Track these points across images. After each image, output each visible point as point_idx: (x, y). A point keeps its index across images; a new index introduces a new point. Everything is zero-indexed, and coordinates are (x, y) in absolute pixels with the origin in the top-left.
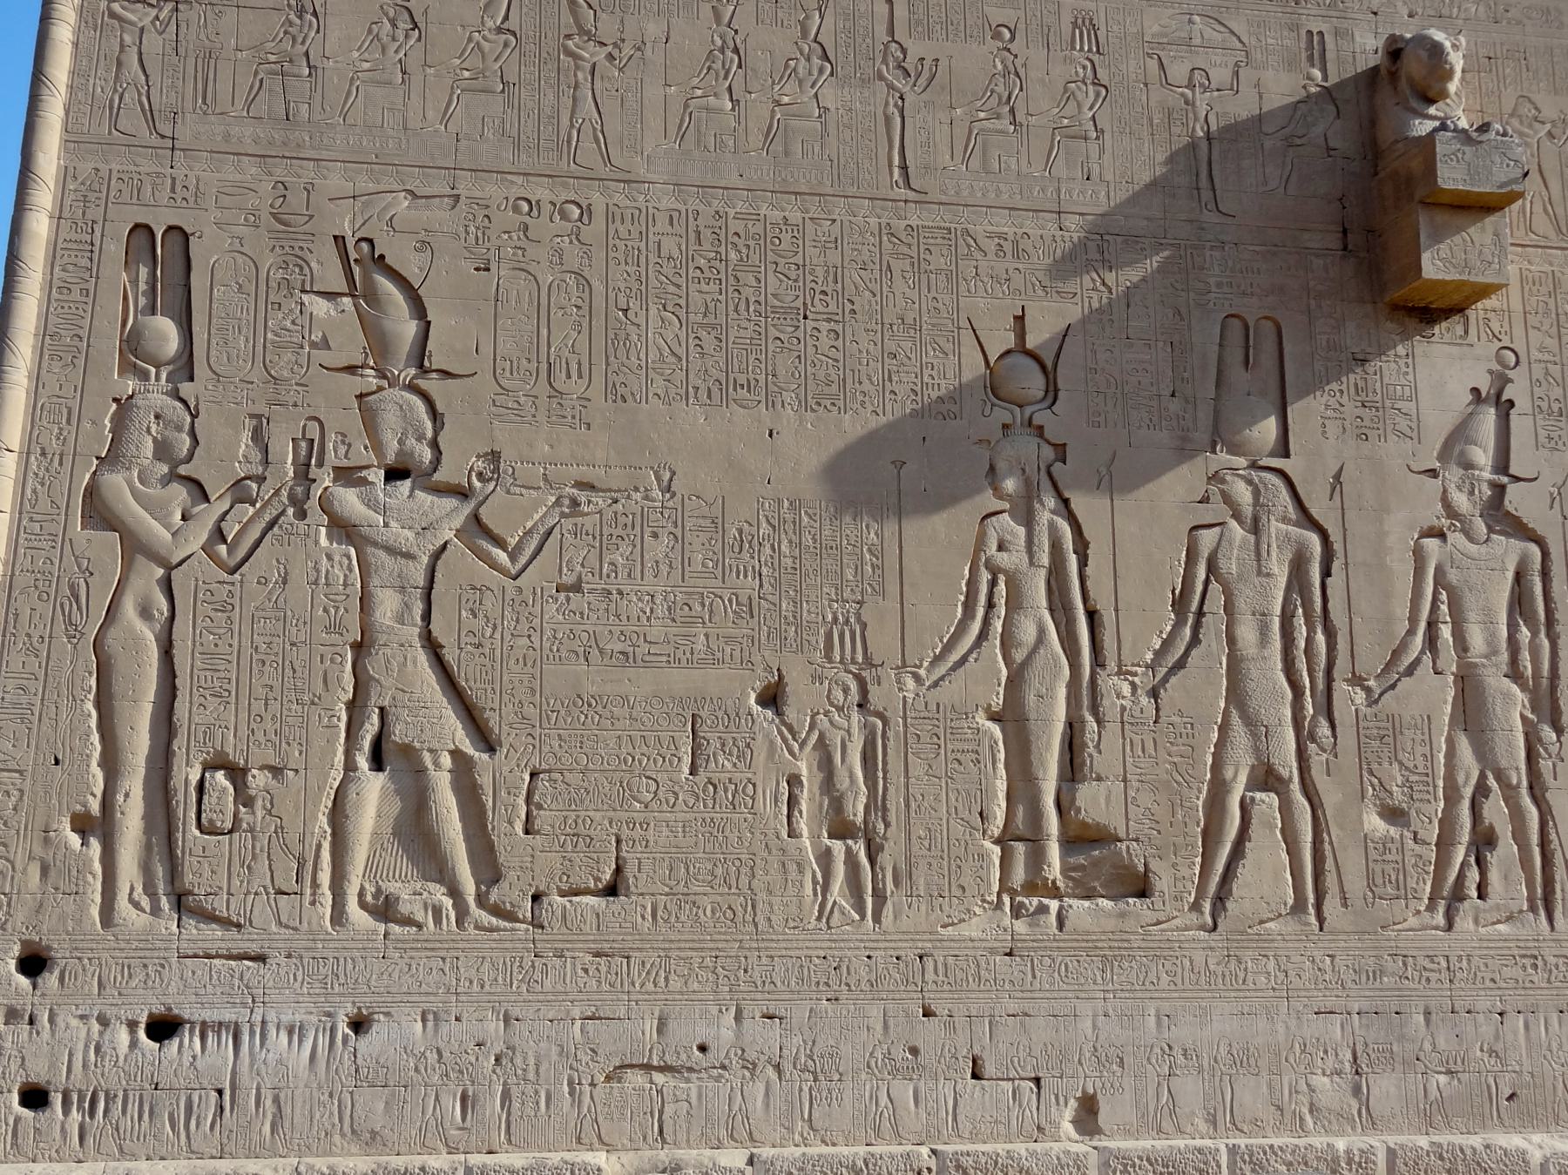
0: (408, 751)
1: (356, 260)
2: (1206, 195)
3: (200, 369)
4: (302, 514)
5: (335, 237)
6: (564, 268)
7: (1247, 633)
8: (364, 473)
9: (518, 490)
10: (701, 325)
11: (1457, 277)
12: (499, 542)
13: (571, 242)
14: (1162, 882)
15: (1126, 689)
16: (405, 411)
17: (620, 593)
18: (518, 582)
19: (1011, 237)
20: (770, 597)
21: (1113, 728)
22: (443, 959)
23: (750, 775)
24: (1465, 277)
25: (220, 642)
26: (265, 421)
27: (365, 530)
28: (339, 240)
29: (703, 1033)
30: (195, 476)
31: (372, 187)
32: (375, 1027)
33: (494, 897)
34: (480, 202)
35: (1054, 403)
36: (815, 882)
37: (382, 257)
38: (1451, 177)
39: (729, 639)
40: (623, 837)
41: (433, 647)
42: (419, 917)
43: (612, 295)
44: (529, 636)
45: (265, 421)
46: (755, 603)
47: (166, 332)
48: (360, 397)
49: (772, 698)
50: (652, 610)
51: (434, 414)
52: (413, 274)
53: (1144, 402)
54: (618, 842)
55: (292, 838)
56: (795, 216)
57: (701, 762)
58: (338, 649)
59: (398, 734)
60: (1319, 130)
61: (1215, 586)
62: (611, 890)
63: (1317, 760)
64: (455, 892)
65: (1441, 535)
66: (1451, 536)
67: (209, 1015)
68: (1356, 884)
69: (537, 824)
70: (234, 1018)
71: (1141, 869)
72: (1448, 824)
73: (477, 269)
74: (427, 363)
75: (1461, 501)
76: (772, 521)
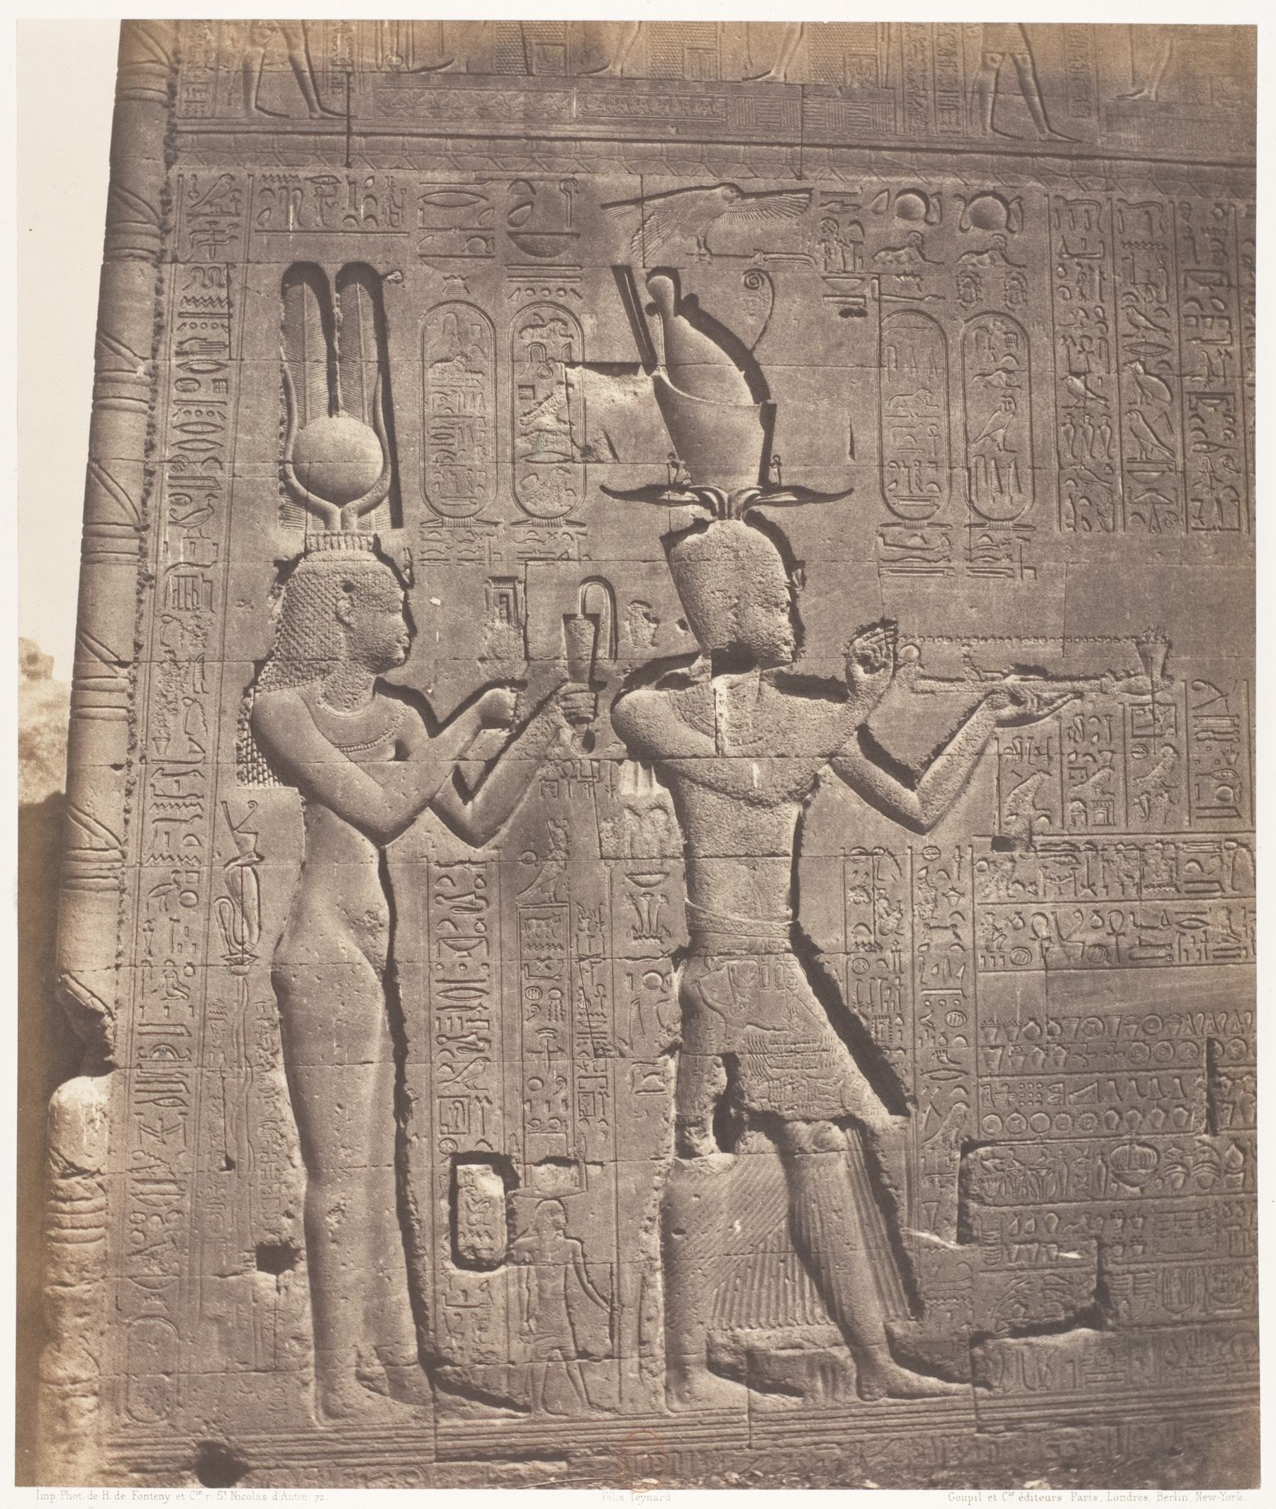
1: (652, 309)
3: (415, 509)
4: (589, 742)
13: (993, 260)
16: (740, 558)
17: (1092, 846)
25: (468, 960)
26: (520, 587)
28: (623, 273)
34: (847, 200)
37: (693, 299)
41: (803, 947)
43: (1061, 351)
45: (520, 587)
48: (671, 539)
50: (1142, 877)
51: (791, 564)
52: (745, 324)
55: (598, 1271)
73: (845, 314)
74: (773, 478)
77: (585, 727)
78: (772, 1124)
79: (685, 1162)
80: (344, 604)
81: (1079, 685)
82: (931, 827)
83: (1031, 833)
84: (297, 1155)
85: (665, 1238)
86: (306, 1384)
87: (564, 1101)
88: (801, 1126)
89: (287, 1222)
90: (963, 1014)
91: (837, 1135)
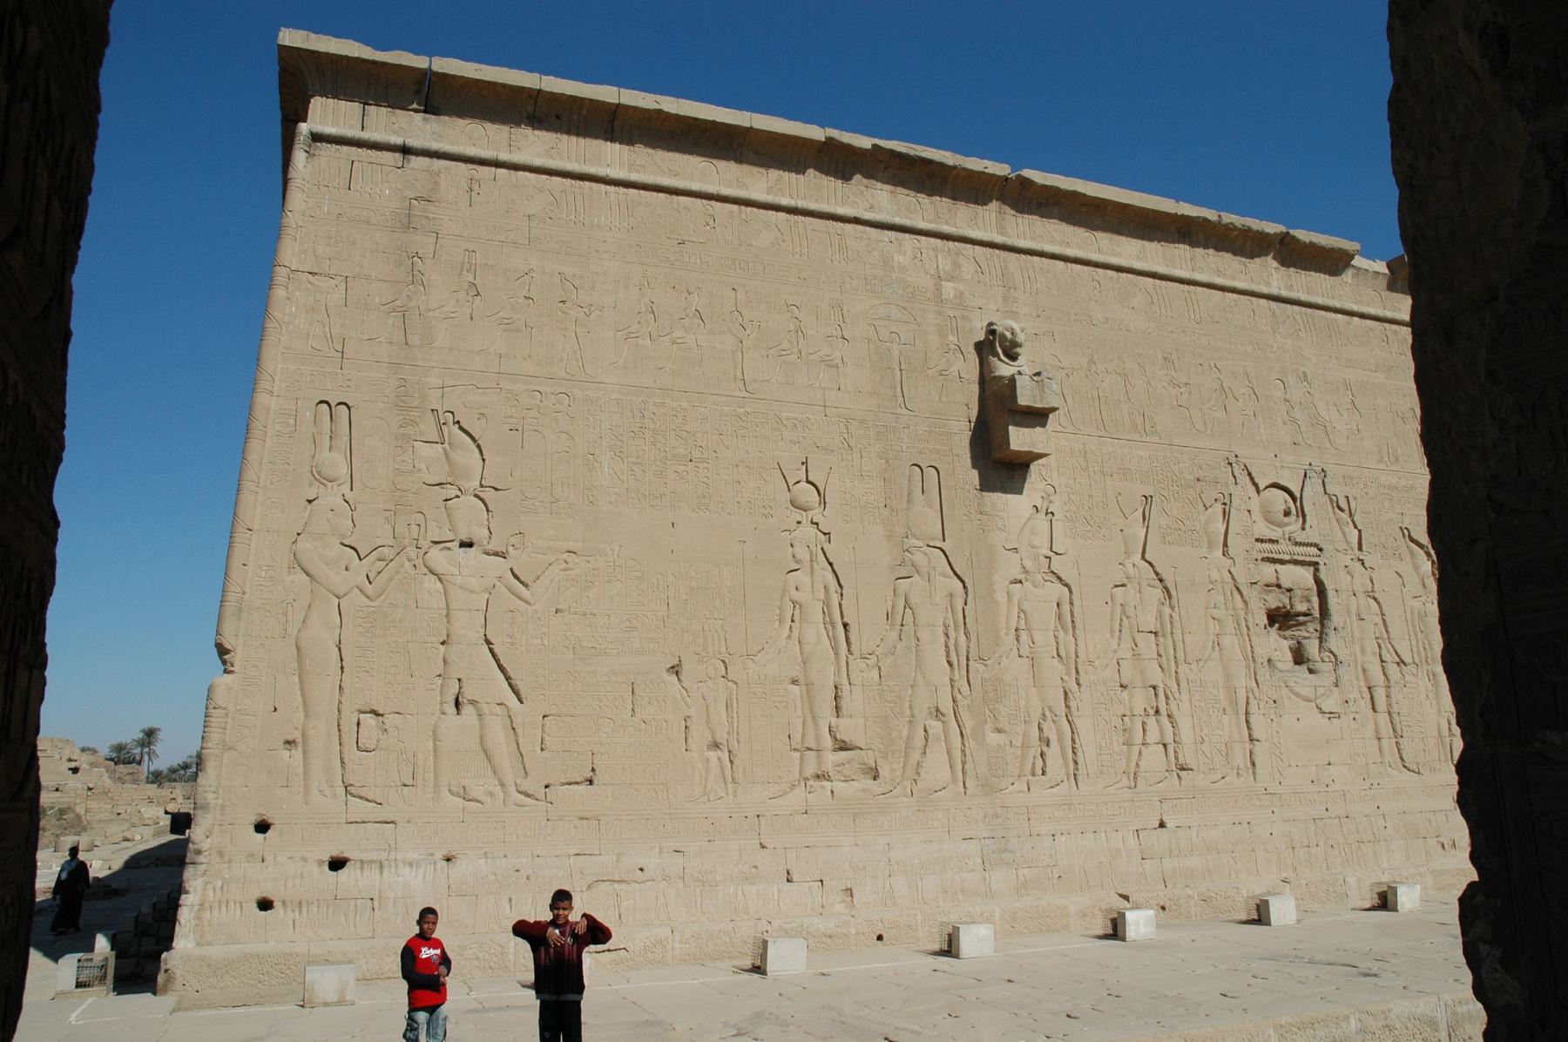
0: (472, 702)
1: (444, 424)
2: (900, 400)
5: (433, 410)
6: (560, 430)
7: (924, 635)
8: (448, 545)
9: (535, 555)
10: (635, 463)
11: (1027, 449)
12: (526, 585)
14: (884, 772)
18: (534, 607)
19: (800, 419)
22: (497, 822)
23: (664, 717)
24: (1031, 450)
26: (393, 513)
27: (450, 578)
29: (642, 862)
30: (352, 545)
31: (453, 383)
32: (459, 861)
33: (523, 789)
36: (701, 776)
37: (458, 422)
38: (1024, 399)
40: (595, 752)
41: (488, 642)
42: (482, 798)
44: (541, 638)
46: (666, 618)
47: (336, 462)
49: (676, 670)
50: (609, 624)
54: (593, 754)
56: (685, 405)
58: (435, 645)
59: (468, 693)
60: (955, 368)
61: (908, 610)
62: (591, 782)
63: (962, 703)
64: (502, 785)
65: (1021, 582)
66: (1025, 583)
67: (364, 856)
69: (548, 744)
70: (379, 858)
71: (874, 765)
72: (1026, 735)
73: (511, 430)
75: (1029, 564)
77: (413, 563)
78: (472, 702)
79: (442, 716)
80: (330, 516)
81: (587, 558)
82: (535, 604)
83: (570, 607)
84: (301, 708)
85: (435, 744)
86: (299, 793)
87: (400, 692)
88: (485, 705)
89: (296, 732)
90: (544, 669)
91: (498, 709)
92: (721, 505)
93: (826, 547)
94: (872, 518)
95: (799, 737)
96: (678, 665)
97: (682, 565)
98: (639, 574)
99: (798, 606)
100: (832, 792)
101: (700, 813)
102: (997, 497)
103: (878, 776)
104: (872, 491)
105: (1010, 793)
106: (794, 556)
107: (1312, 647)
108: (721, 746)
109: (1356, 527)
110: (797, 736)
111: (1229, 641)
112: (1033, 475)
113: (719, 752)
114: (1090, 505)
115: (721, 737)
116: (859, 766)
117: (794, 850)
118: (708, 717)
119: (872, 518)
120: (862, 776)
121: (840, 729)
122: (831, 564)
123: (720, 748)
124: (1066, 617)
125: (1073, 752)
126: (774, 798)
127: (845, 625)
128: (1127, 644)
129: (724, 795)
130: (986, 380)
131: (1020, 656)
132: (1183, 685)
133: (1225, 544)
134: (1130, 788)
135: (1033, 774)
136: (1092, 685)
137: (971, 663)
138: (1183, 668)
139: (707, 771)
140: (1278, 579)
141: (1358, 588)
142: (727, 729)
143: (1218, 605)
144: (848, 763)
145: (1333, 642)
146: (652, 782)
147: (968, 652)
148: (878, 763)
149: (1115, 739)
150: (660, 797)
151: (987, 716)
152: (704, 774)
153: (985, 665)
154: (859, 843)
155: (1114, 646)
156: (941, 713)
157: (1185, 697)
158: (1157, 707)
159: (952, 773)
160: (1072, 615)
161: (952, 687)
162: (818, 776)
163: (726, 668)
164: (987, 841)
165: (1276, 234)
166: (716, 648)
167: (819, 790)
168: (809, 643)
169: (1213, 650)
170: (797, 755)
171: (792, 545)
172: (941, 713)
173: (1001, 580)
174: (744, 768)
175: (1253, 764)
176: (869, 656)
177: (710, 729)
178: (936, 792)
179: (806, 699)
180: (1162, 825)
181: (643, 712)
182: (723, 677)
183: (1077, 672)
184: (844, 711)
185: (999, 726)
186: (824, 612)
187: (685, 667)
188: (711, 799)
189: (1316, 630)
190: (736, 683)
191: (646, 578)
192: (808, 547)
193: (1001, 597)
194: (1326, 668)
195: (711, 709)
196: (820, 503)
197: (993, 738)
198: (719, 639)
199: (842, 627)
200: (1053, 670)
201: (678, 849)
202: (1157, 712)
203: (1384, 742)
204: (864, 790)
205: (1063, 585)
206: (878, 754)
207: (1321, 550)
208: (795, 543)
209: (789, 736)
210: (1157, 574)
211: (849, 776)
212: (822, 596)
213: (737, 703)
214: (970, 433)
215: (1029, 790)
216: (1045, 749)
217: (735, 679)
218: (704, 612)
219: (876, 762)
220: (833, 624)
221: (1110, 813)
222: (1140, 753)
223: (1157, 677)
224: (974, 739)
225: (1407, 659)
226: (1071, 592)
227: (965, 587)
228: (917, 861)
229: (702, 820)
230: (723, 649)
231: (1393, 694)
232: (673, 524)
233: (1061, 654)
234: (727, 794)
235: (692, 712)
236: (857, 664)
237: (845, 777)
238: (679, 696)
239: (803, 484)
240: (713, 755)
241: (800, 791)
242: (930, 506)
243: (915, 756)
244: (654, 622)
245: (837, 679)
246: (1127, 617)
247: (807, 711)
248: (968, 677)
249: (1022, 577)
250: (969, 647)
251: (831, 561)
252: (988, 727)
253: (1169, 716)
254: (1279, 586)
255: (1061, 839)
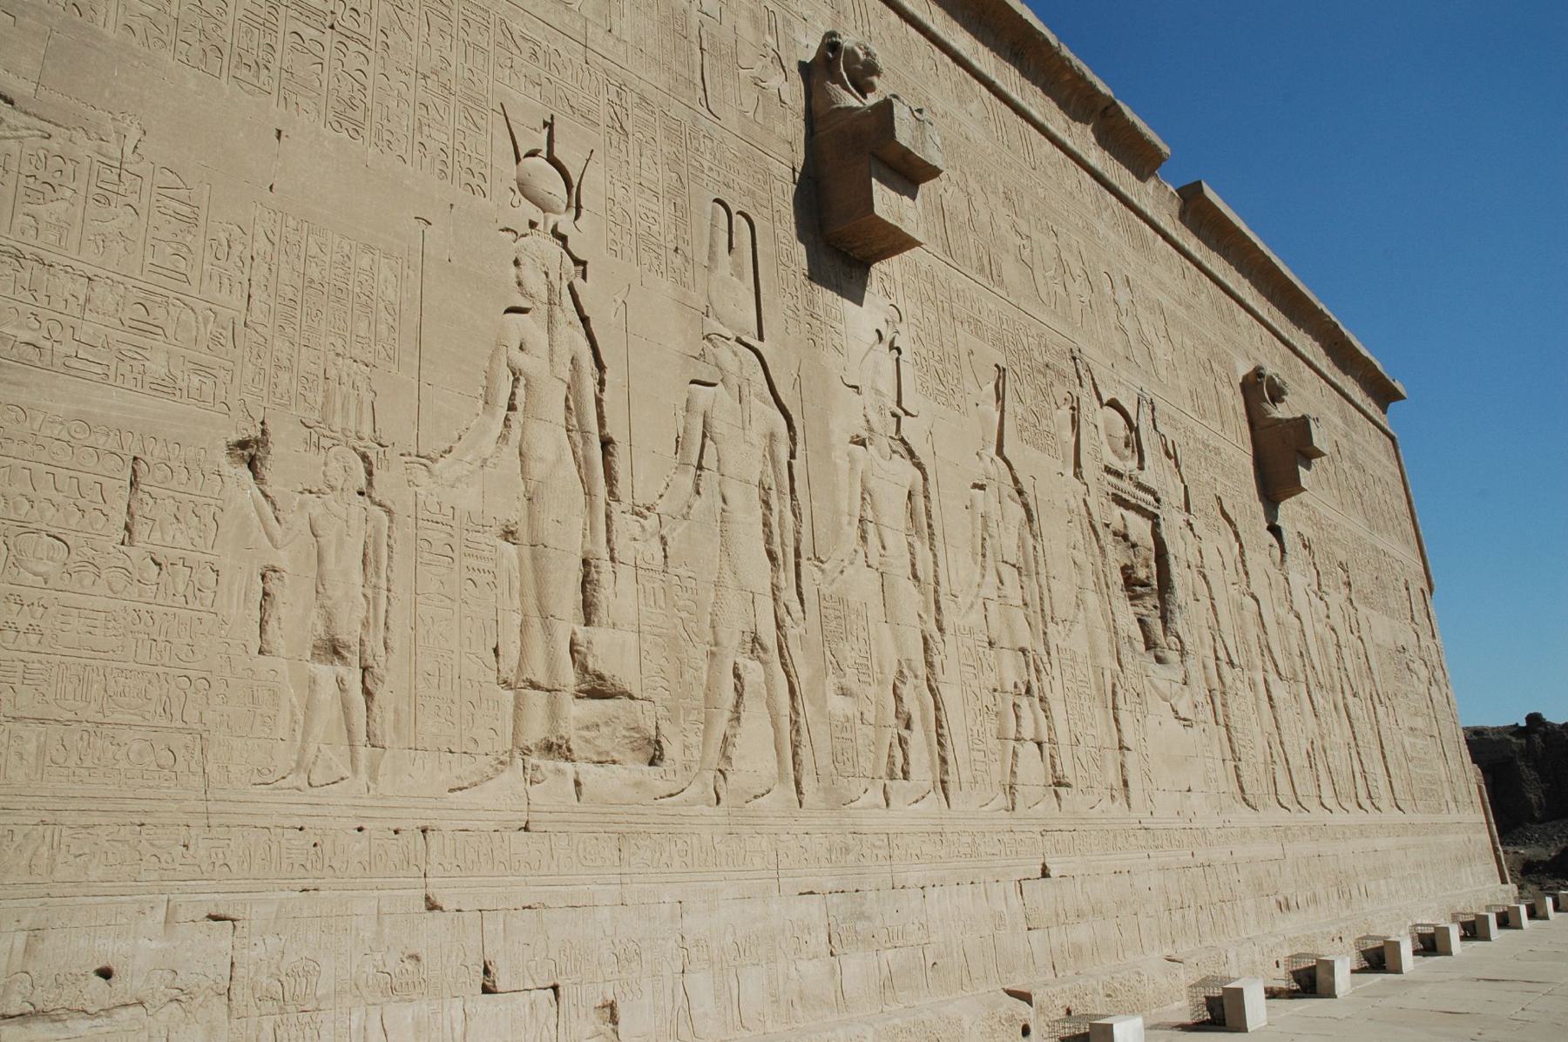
14: (672, 750)
15: (637, 531)
20: (260, 328)
21: (625, 572)
35: (577, 217)
39: (200, 369)
49: (250, 453)
53: (652, 247)
57: (141, 530)
63: (793, 632)
68: (825, 761)
76: (271, 236)
92: (387, 136)
93: (578, 283)
94: (655, 262)
95: (516, 655)
96: (257, 441)
97: (292, 223)
98: (185, 210)
99: (523, 381)
100: (577, 784)
101: (287, 816)
102: (827, 297)
103: (661, 758)
104: (656, 216)
105: (864, 808)
106: (520, 284)
107: (1157, 626)
108: (345, 653)
109: (1183, 481)
110: (511, 652)
111: (1092, 599)
112: (874, 283)
113: (341, 669)
114: (941, 354)
115: (348, 631)
116: (625, 733)
117: (501, 915)
118: (321, 577)
119: (655, 262)
120: (630, 755)
121: (596, 650)
122: (585, 320)
123: (343, 658)
124: (922, 522)
125: (940, 743)
126: (460, 789)
127: (606, 443)
128: (992, 578)
129: (347, 773)
130: (817, 117)
131: (868, 566)
132: (1053, 652)
133: (1077, 464)
134: (1008, 811)
135: (892, 777)
136: (958, 634)
137: (803, 562)
138: (1051, 625)
139: (309, 707)
140: (1125, 526)
141: (1193, 563)
142: (363, 614)
143: (1078, 545)
144: (606, 724)
145: (1179, 624)
146: (164, 723)
147: (798, 541)
148: (663, 731)
149: (988, 726)
150: (181, 766)
151: (828, 663)
152: (301, 718)
153: (823, 571)
154: (628, 901)
155: (978, 579)
156: (761, 645)
157: (1056, 672)
158: (1029, 682)
159: (779, 762)
160: (929, 516)
161: (775, 600)
162: (549, 747)
163: (370, 473)
164: (836, 898)
165: (1105, 95)
166: (352, 425)
167: (550, 776)
168: (541, 459)
169: (1078, 609)
170: (510, 694)
171: (517, 263)
172: (761, 645)
173: (840, 435)
174: (396, 711)
175: (1126, 783)
176: (646, 512)
177: (322, 606)
178: (755, 797)
179: (530, 576)
180: (1045, 873)
181: (157, 535)
182: (361, 493)
183: (938, 609)
184: (602, 614)
185: (845, 682)
186: (568, 408)
187: (276, 448)
188: (315, 780)
189: (1155, 607)
190: (389, 512)
191: (202, 221)
192: (547, 274)
193: (843, 464)
194: (1173, 656)
195: (330, 556)
196: (568, 206)
197: (837, 704)
198: (360, 409)
199: (599, 444)
200: (910, 599)
201: (221, 912)
202: (1028, 691)
203: (1227, 762)
204: (638, 785)
205: (914, 464)
206: (661, 711)
207: (1158, 500)
208: (524, 260)
209: (496, 651)
210: (1016, 481)
211: (608, 753)
212: (567, 376)
213: (390, 557)
214: (795, 186)
215: (888, 805)
216: (905, 733)
217: (388, 503)
218: (332, 339)
219: (657, 728)
220: (584, 433)
221: (989, 850)
222: (1014, 752)
223: (1025, 639)
224: (812, 703)
225: (1236, 661)
226: (925, 479)
227: (791, 427)
228: (729, 939)
229: (290, 834)
230: (366, 430)
231: (1229, 701)
232: (279, 132)
233: (919, 574)
234: (355, 771)
235: (282, 559)
236: (625, 524)
237: (599, 754)
238: (254, 515)
239: (540, 162)
240: (325, 672)
241: (512, 776)
242: (740, 277)
243: (721, 725)
244: (210, 327)
245: (588, 546)
246: (990, 536)
247: (532, 601)
248: (798, 586)
249: (865, 434)
250: (799, 533)
251: (587, 312)
252: (831, 681)
253: (1041, 700)
254: (1125, 537)
255: (933, 894)
